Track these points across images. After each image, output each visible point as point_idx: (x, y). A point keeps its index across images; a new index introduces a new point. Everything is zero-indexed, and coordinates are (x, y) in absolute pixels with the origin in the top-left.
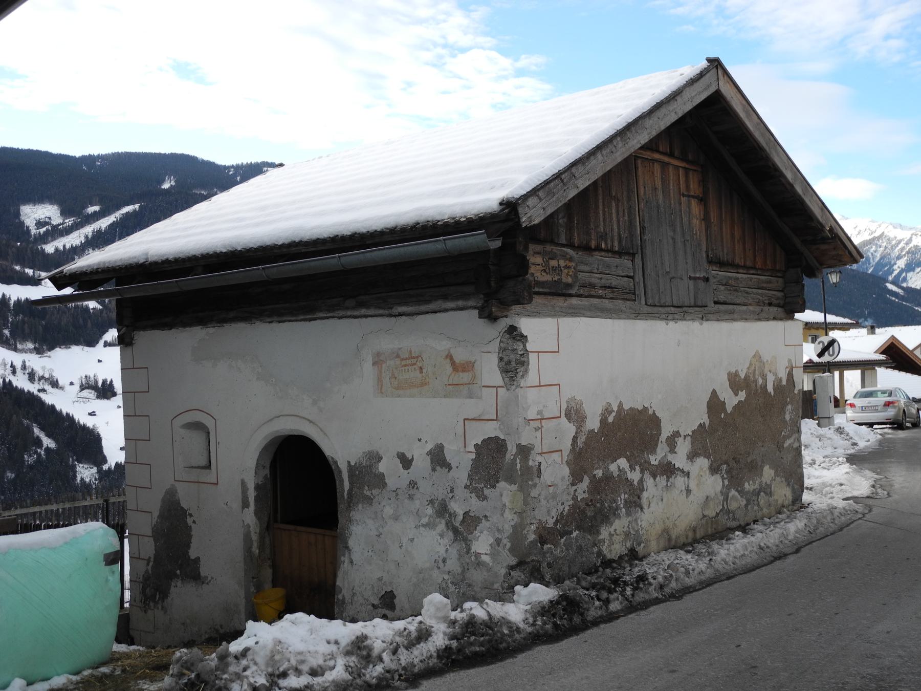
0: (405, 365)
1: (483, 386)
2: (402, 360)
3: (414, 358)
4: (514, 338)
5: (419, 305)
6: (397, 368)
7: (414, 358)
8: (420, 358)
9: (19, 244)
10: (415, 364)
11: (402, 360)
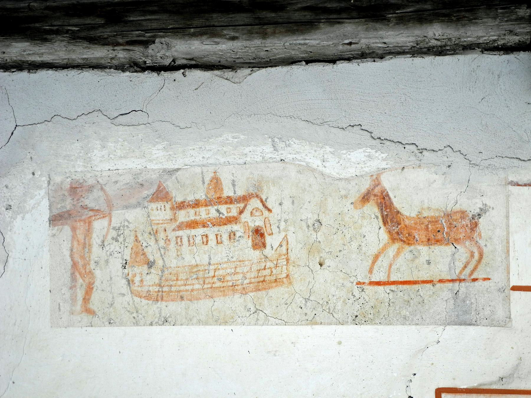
0: (192, 225)
1: (515, 288)
2: (182, 206)
3: (230, 201)
4: (377, 55)
5: (264, 35)
6: (154, 233)
7: (230, 201)
8: (255, 203)
9: (11, 21)
10: (230, 220)
11: (182, 206)
